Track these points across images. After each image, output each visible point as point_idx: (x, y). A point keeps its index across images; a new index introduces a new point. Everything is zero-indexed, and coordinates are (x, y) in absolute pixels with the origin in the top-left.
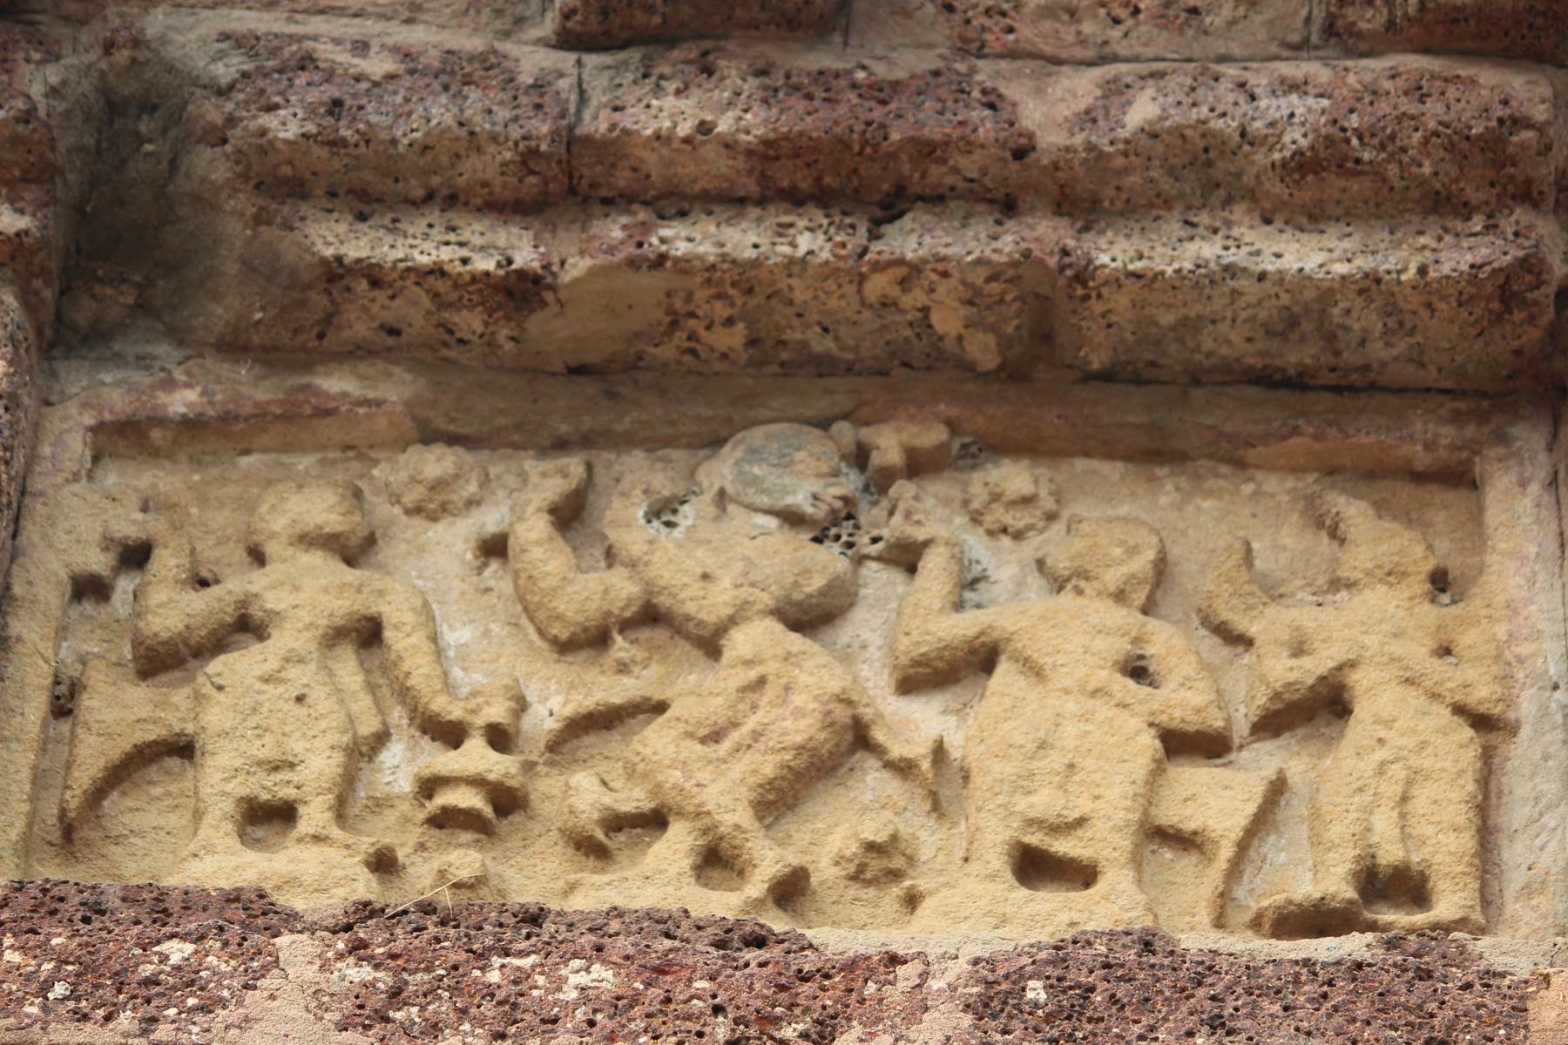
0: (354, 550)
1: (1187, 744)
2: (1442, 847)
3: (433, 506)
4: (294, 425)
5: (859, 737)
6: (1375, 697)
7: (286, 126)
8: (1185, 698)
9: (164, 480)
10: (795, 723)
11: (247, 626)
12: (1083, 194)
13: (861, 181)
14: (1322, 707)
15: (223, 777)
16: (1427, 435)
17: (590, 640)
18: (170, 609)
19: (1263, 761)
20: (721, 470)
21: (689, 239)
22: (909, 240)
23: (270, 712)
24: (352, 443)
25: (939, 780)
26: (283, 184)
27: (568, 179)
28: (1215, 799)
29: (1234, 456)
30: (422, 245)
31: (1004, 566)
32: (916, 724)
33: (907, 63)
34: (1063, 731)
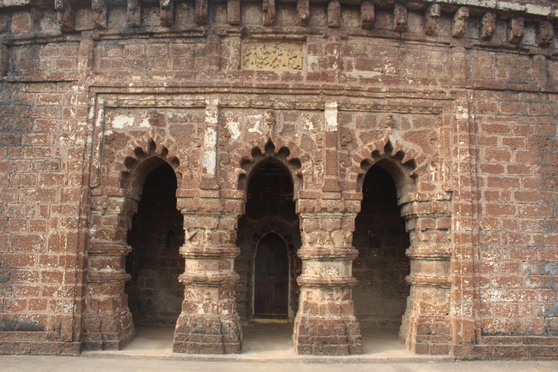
0: (255, 49)
1: (290, 59)
2: (301, 65)
3: (258, 46)
4: (252, 42)
5: (276, 59)
6: (298, 57)
7: (252, 31)
8: (290, 57)
9: (247, 45)
10: (274, 59)
11: (251, 53)
12: (286, 33)
13: (277, 33)
14: (296, 57)
15: (250, 62)
16: (300, 42)
17: (265, 53)
18: (248, 53)
19: (294, 59)
20: (270, 45)
21: (269, 35)
22: (279, 35)
23: (252, 58)
24: (255, 43)
25: (280, 61)
26: (251, 33)
27: (264, 33)
28: (291, 62)
29: (292, 43)
30: (258, 36)
31: (282, 49)
32: (279, 58)
33: (278, 27)
34: (285, 59)
